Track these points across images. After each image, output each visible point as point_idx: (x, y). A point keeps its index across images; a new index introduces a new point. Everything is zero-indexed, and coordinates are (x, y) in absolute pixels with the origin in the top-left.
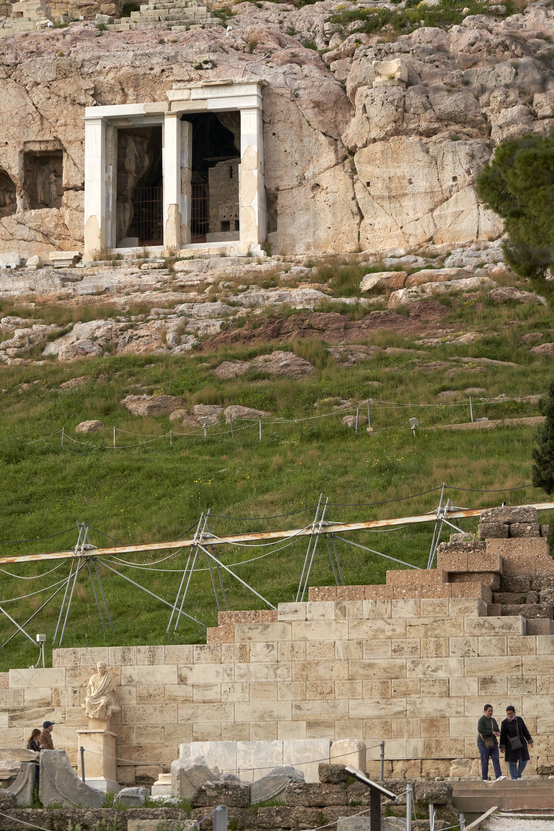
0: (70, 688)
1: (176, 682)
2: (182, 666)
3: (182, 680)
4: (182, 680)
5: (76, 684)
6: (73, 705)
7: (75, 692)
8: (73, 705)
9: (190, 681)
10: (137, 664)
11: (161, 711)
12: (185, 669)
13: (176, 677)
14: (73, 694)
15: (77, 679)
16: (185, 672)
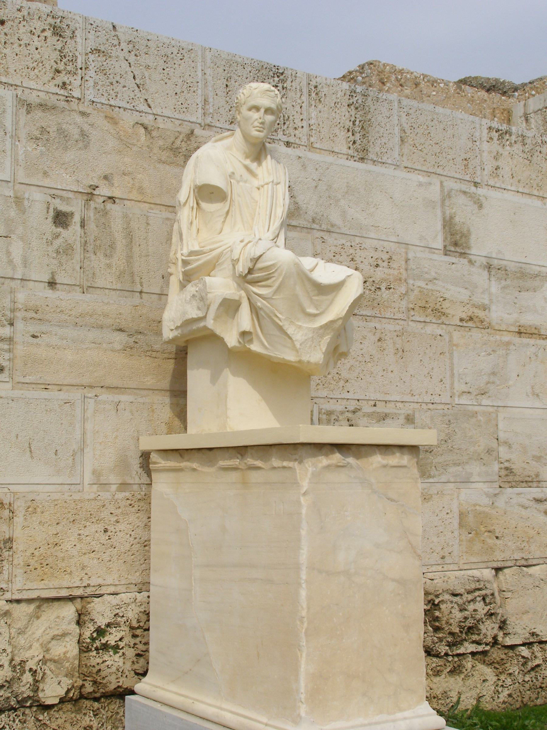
0: (38, 196)
1: (439, 244)
2: (457, 186)
3: (456, 242)
4: (456, 242)
5: (65, 180)
6: (52, 284)
7: (61, 219)
8: (52, 284)
9: (479, 249)
10: (311, 147)
11: (400, 353)
12: (462, 200)
13: (439, 225)
14: (49, 227)
15: (70, 156)
16: (463, 212)
